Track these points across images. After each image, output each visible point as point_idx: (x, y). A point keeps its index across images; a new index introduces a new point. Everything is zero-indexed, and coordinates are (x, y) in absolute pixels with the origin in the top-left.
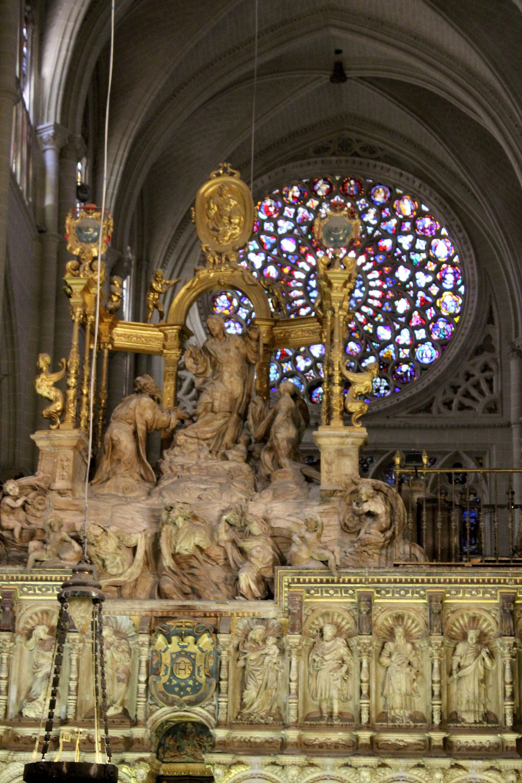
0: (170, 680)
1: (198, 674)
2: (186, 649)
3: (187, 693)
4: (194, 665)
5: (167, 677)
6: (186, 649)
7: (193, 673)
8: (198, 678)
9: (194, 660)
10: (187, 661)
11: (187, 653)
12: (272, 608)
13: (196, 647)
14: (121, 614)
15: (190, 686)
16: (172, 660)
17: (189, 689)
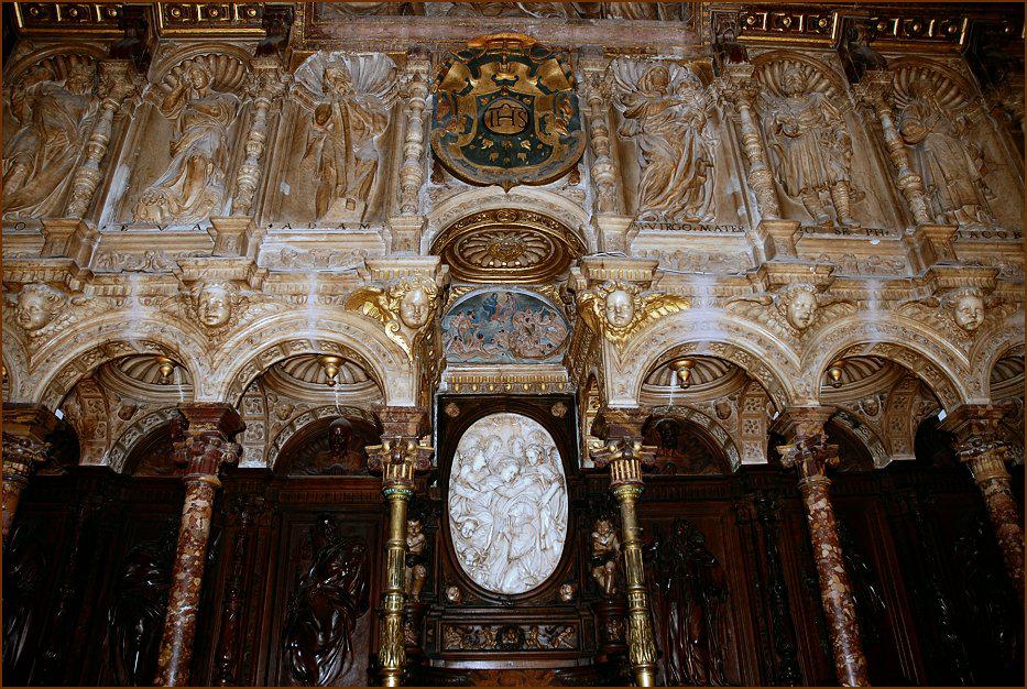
0: (476, 142)
1: (542, 129)
2: (511, 88)
3: (518, 163)
4: (530, 115)
5: (471, 136)
6: (511, 88)
7: (529, 126)
8: (540, 136)
9: (531, 106)
10: (514, 104)
11: (513, 95)
12: (680, 37)
13: (533, 83)
14: (369, 49)
15: (524, 150)
16: (480, 107)
17: (522, 156)
